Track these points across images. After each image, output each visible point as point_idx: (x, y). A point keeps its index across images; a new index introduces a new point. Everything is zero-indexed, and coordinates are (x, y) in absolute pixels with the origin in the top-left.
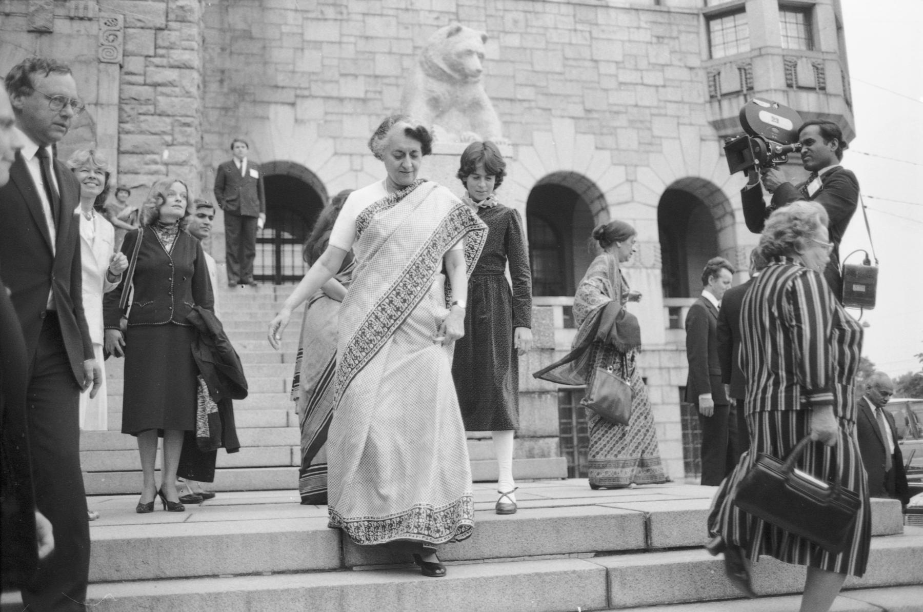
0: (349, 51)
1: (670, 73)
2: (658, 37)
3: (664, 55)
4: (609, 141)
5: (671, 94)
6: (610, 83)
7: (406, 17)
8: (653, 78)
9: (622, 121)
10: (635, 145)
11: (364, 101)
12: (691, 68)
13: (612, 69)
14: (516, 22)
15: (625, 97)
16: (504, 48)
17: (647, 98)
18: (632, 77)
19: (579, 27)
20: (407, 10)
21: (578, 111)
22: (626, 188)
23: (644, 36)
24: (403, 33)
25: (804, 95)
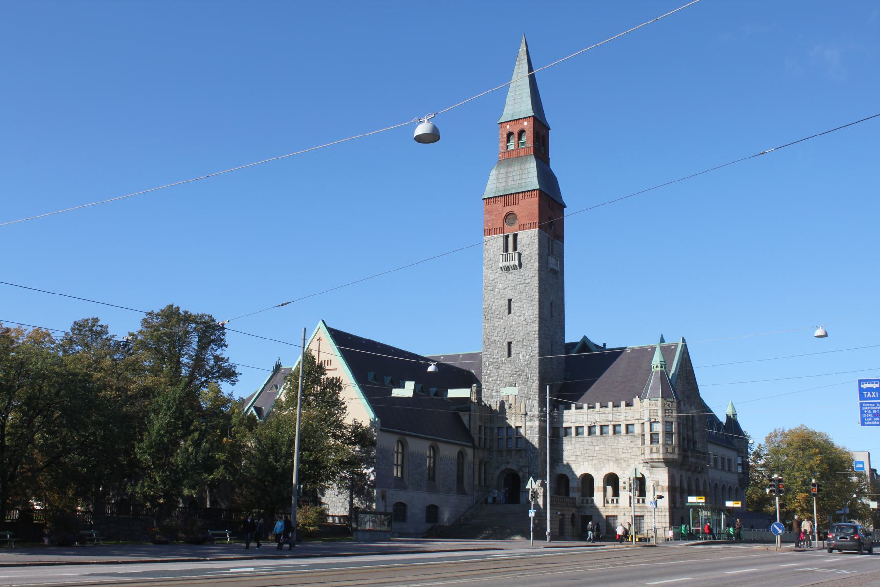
0: (572, 451)
1: (633, 449)
2: (632, 441)
3: (632, 445)
4: (620, 465)
5: (632, 454)
6: (621, 453)
7: (583, 443)
8: (629, 451)
9: (623, 461)
10: (625, 466)
11: (575, 461)
12: (638, 448)
13: (621, 450)
14: (603, 442)
15: (624, 455)
16: (600, 448)
17: (628, 455)
18: (626, 451)
19: (615, 441)
20: (582, 441)
21: (614, 459)
22: (623, 475)
23: (629, 441)
24: (582, 446)
25: (654, 454)
